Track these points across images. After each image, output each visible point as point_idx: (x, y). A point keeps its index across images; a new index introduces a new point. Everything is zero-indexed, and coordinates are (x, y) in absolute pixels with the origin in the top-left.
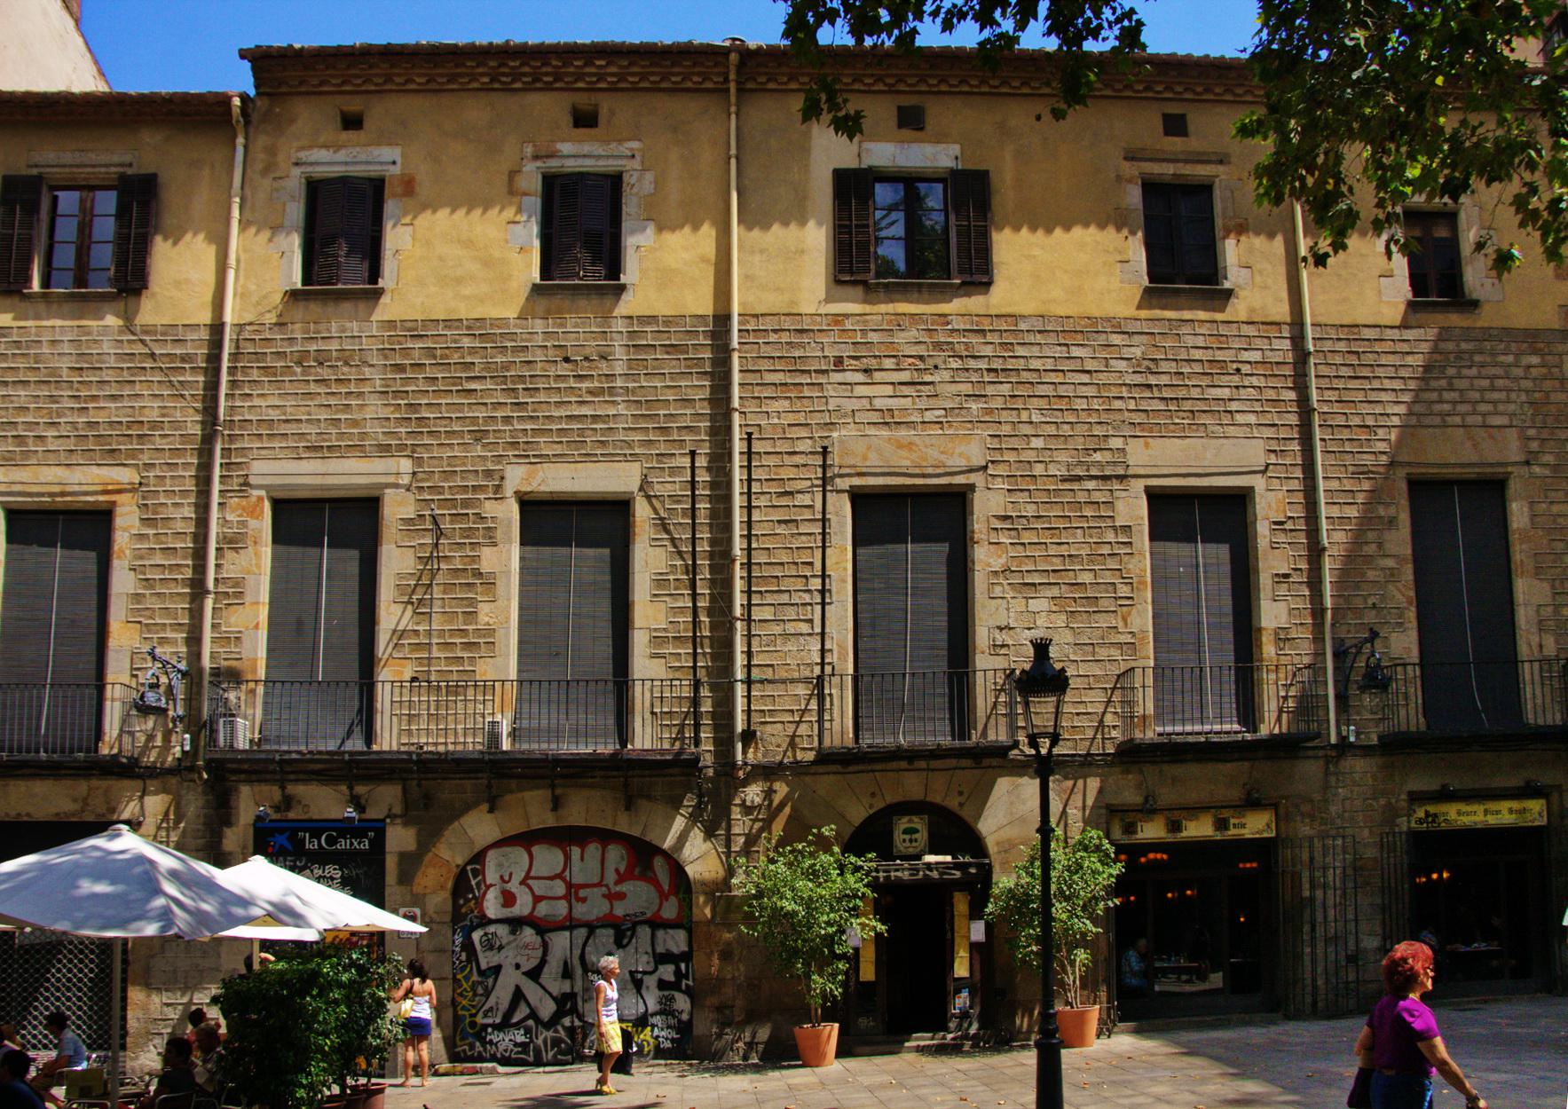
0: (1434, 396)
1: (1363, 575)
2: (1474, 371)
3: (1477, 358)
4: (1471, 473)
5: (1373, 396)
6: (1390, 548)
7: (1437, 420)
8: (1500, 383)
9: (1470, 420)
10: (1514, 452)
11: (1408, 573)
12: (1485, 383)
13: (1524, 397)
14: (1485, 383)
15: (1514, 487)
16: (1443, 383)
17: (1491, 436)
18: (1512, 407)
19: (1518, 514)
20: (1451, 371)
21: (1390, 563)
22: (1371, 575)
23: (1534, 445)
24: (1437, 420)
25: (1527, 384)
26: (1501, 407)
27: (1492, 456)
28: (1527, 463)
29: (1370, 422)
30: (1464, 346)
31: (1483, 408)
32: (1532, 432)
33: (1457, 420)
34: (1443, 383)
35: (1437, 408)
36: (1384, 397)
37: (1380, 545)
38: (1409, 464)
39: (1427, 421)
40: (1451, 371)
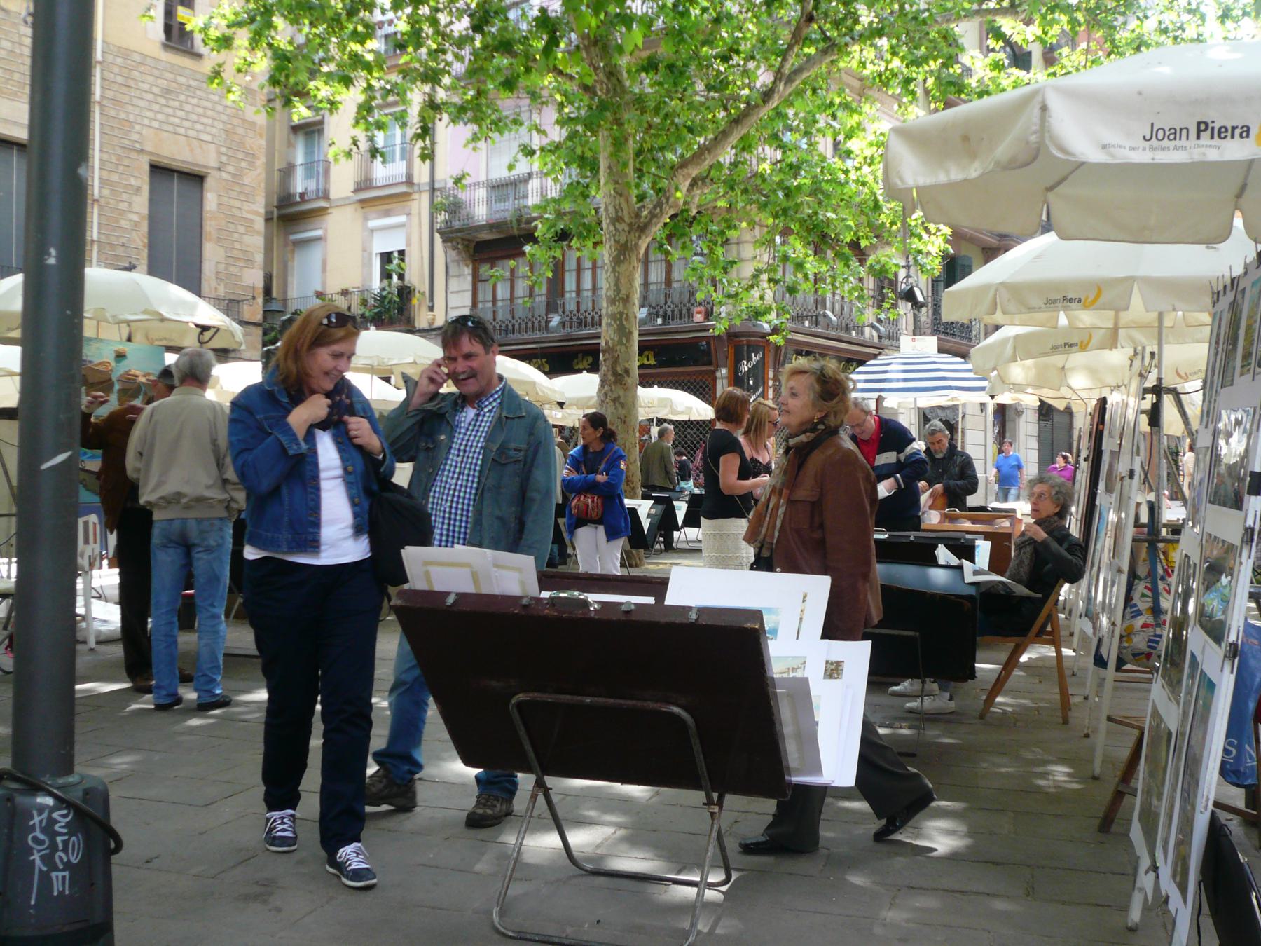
0: (170, 111)
1: (117, 221)
2: (194, 101)
3: (198, 92)
4: (187, 168)
5: (135, 101)
6: (136, 208)
7: (170, 128)
8: (209, 113)
9: (191, 133)
10: (213, 163)
11: (145, 227)
12: (200, 111)
13: (221, 126)
14: (200, 111)
15: (209, 183)
16: (176, 104)
17: (201, 147)
18: (214, 131)
19: (211, 200)
20: (182, 98)
21: (135, 217)
22: (123, 223)
23: (224, 159)
24: (170, 128)
25: (224, 118)
26: (209, 129)
27: (200, 160)
28: (219, 169)
29: (131, 118)
30: (192, 83)
31: (198, 127)
32: (223, 150)
33: (182, 131)
34: (176, 104)
35: (172, 120)
36: (142, 103)
37: (130, 204)
38: (151, 153)
39: (166, 127)
40: (182, 98)
